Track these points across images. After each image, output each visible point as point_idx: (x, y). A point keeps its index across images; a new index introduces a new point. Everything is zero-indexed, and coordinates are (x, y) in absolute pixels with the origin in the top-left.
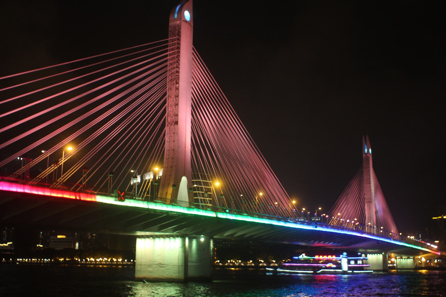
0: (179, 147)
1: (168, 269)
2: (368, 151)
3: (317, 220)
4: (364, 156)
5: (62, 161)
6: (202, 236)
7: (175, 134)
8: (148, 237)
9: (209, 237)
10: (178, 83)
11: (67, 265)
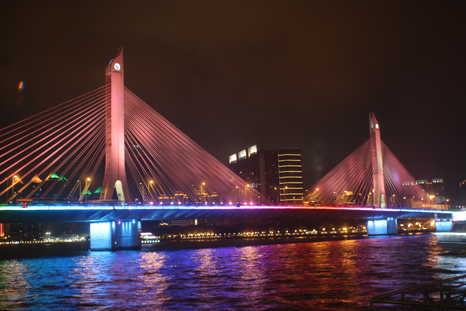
0: (113, 161)
2: (374, 126)
3: (435, 182)
4: (371, 131)
5: (14, 184)
8: (95, 222)
9: (138, 220)
10: (111, 117)
11: (174, 241)
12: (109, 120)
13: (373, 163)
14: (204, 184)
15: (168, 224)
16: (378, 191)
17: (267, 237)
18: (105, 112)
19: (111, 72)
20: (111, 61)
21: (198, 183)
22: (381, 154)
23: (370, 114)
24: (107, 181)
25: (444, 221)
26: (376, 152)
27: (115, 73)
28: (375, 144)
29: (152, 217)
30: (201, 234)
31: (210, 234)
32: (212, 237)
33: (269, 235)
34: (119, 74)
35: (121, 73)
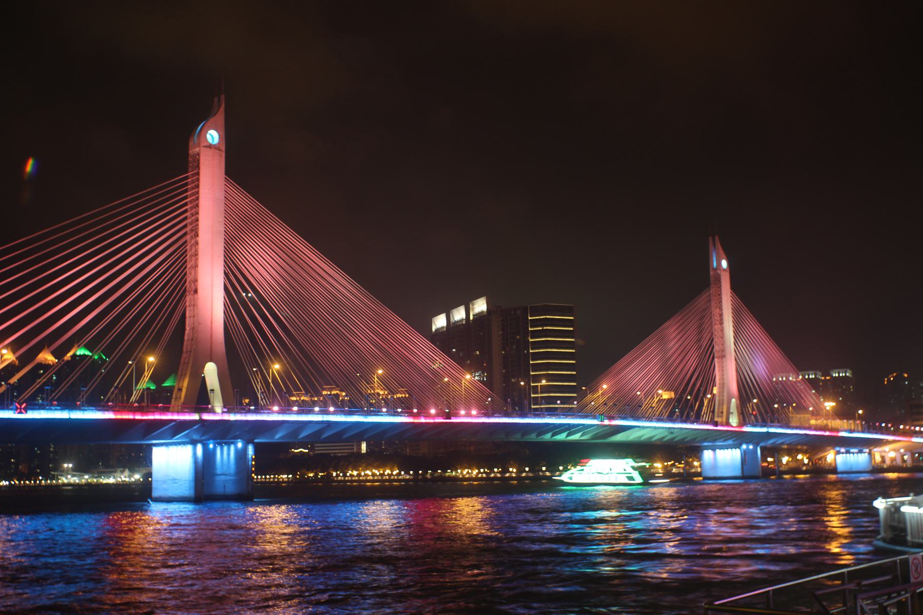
0: (200, 324)
1: (180, 485)
2: (719, 264)
3: (837, 375)
4: (712, 273)
6: (239, 440)
7: (195, 307)
8: (162, 445)
9: (247, 442)
10: (198, 236)
12: (193, 241)
13: (715, 335)
14: (380, 372)
15: (307, 451)
16: (723, 392)
17: (503, 479)
18: (185, 226)
19: (199, 145)
20: (201, 125)
21: (370, 370)
22: (731, 319)
23: (710, 239)
24: (188, 363)
25: (853, 453)
26: (721, 315)
27: (208, 149)
28: (721, 298)
29: (277, 436)
30: (374, 471)
31: (392, 472)
32: (396, 477)
33: (507, 475)
34: (218, 151)
35: (220, 150)
